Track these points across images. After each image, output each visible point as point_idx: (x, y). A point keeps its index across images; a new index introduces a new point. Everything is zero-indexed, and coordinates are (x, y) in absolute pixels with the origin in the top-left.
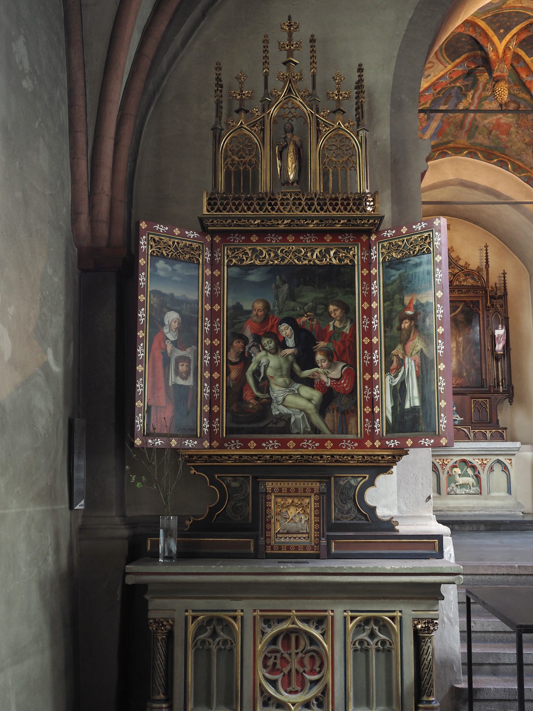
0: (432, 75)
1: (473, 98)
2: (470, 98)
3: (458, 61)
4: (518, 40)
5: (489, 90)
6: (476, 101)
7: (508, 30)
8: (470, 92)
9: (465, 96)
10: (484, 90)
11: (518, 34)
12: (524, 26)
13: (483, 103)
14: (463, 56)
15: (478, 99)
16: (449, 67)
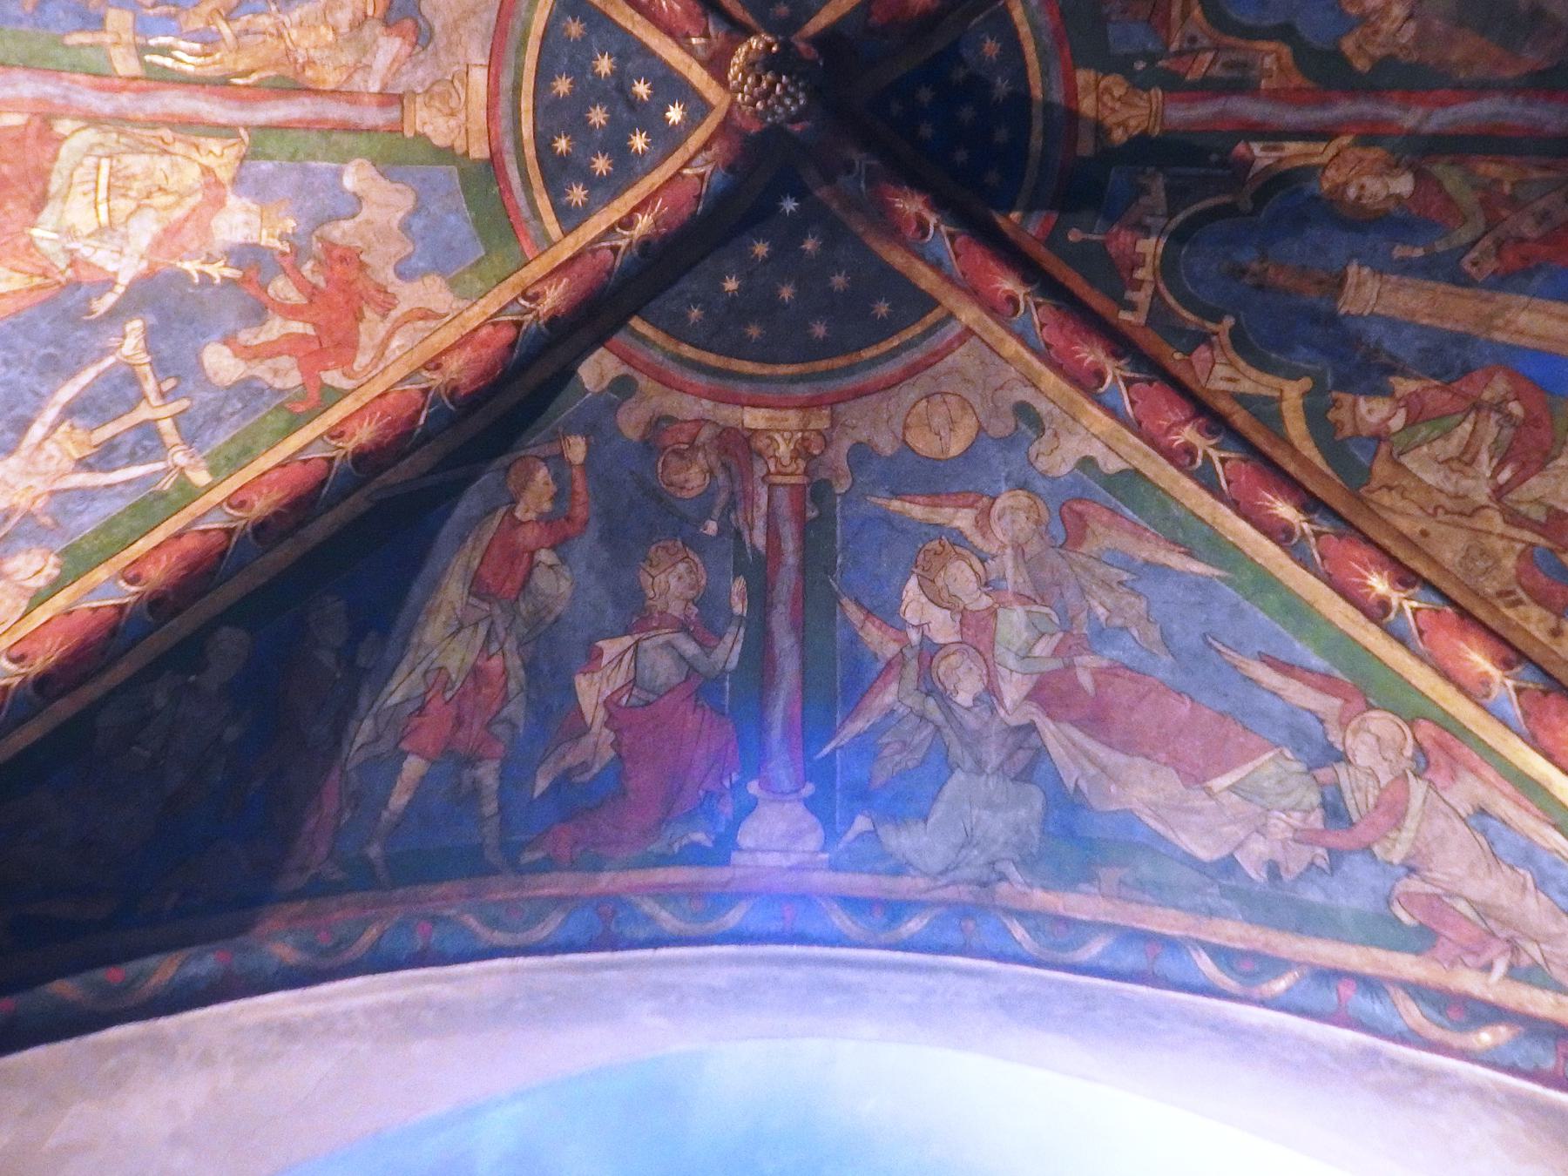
0: (1024, 394)
1: (1323, 134)
2: (1321, 147)
3: (926, 279)
4: (688, 27)
5: (1241, 57)
6: (1344, 109)
7: (671, 85)
8: (1248, 163)
9: (1283, 180)
10: (1240, 84)
11: (670, 32)
12: (638, 17)
13: (1362, 65)
14: (897, 258)
15: (1323, 103)
16: (969, 314)
